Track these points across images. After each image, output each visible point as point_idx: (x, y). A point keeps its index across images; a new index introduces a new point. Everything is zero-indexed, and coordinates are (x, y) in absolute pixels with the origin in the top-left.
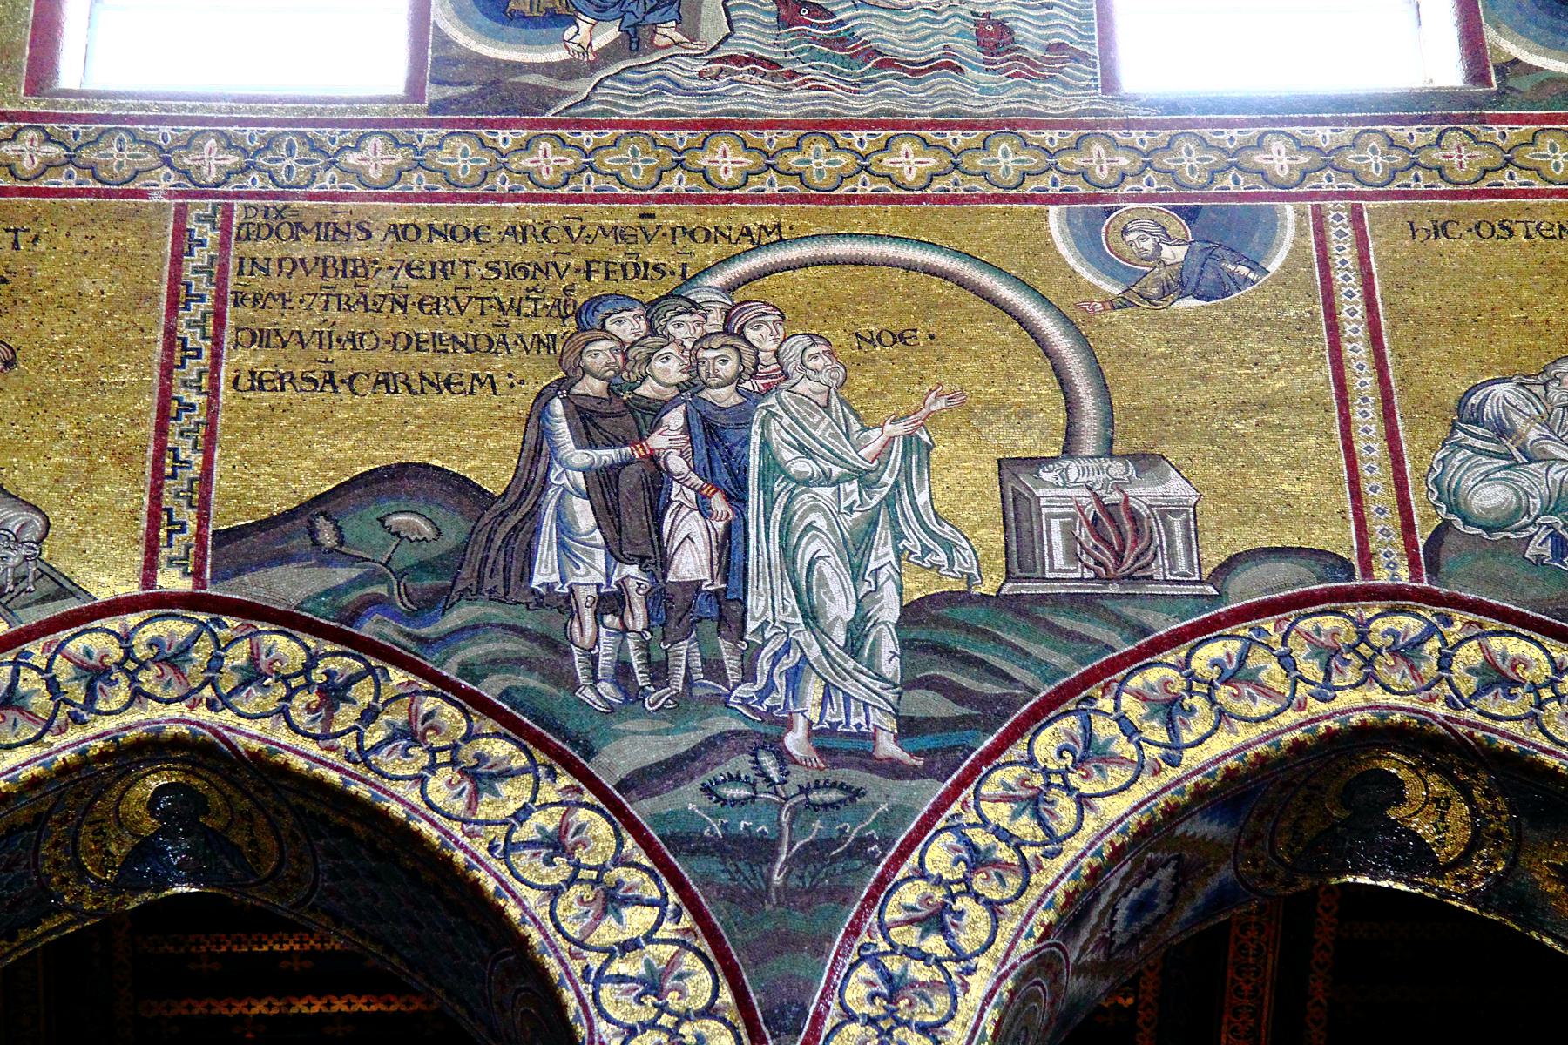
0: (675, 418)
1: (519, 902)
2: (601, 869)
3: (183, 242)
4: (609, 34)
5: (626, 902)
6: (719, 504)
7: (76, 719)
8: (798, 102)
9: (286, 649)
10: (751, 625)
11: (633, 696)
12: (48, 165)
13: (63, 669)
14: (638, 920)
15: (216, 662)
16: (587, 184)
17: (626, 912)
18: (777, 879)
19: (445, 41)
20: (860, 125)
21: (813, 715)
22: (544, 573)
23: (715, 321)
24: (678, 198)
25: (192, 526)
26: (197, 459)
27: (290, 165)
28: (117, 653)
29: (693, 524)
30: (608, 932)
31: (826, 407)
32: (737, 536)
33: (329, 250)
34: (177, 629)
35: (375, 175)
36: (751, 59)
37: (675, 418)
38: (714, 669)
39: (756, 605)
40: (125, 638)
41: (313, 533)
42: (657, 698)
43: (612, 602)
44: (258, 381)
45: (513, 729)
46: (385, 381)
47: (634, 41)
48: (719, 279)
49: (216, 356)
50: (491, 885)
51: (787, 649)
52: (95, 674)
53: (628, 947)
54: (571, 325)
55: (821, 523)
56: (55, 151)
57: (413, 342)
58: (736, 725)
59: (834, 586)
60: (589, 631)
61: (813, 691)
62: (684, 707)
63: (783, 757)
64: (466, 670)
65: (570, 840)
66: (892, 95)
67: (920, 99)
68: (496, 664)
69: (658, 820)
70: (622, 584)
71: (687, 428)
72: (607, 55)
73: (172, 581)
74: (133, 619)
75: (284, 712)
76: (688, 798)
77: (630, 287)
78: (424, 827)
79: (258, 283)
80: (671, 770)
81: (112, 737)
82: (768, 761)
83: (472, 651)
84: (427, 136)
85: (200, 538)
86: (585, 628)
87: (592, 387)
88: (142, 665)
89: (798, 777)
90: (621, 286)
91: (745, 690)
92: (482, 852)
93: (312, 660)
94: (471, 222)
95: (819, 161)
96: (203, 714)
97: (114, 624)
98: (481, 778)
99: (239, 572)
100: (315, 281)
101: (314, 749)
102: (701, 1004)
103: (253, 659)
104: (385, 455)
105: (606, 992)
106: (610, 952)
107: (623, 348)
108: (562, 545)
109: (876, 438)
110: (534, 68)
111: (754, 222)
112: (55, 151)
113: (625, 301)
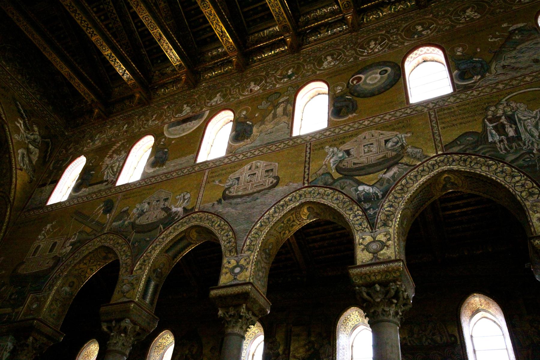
0: (503, 117)
1: (499, 179)
2: (510, 173)
3: (430, 115)
4: (479, 77)
5: (516, 176)
6: (513, 126)
7: (432, 171)
8: (508, 77)
9: (456, 157)
10: (523, 139)
11: (508, 152)
12: (411, 112)
13: (429, 166)
14: (517, 179)
15: (448, 161)
16: (482, 94)
17: (516, 178)
18: (538, 169)
19: (457, 84)
20: (519, 77)
21: (536, 147)
22: (490, 140)
23: (505, 105)
24: (495, 92)
25: (440, 146)
26: (439, 138)
27: (441, 103)
28: (435, 162)
29: (510, 129)
30: (514, 180)
31: (526, 110)
32: (517, 129)
33: (448, 111)
34: (442, 158)
35: (452, 101)
36: (501, 74)
37: (503, 117)
38: (519, 145)
39: (523, 136)
40: (436, 160)
41: (457, 143)
42: (512, 151)
43: (501, 141)
44: (444, 128)
45: (491, 159)
46: (461, 123)
47: (483, 77)
48: (504, 100)
49: (438, 126)
50: (494, 178)
51: (530, 140)
52: (433, 165)
53: (518, 182)
54: (485, 111)
55: (530, 124)
56: (412, 110)
57: (463, 118)
58: (525, 152)
59: (534, 131)
60: (499, 145)
61: (536, 145)
62: (516, 151)
63: (533, 154)
64: (483, 154)
65: (504, 171)
66: (523, 72)
67: (528, 71)
68: (486, 152)
69: (517, 165)
70: (502, 138)
71: (505, 118)
72: (480, 79)
73: (440, 153)
74: (436, 158)
75: (459, 164)
76: (521, 162)
77: (492, 104)
78: (483, 173)
79: (441, 117)
80: (517, 159)
81: (438, 172)
82: (531, 155)
83: (483, 151)
84: (458, 95)
85: (442, 147)
86: (498, 145)
87: (490, 117)
88: (439, 163)
89: (536, 156)
90: (490, 104)
91: (524, 147)
92: (492, 175)
93: (461, 157)
94: (467, 103)
95: (514, 82)
96: (449, 167)
97: (434, 159)
98: (489, 166)
99: (448, 149)
100: (448, 115)
101: (464, 168)
102: (531, 186)
103: (453, 159)
104: (463, 132)
105: (516, 188)
106: (515, 183)
107: (493, 111)
108: (492, 136)
109: (535, 112)
110: (470, 83)
111: (507, 92)
112: (412, 110)
113: (491, 106)
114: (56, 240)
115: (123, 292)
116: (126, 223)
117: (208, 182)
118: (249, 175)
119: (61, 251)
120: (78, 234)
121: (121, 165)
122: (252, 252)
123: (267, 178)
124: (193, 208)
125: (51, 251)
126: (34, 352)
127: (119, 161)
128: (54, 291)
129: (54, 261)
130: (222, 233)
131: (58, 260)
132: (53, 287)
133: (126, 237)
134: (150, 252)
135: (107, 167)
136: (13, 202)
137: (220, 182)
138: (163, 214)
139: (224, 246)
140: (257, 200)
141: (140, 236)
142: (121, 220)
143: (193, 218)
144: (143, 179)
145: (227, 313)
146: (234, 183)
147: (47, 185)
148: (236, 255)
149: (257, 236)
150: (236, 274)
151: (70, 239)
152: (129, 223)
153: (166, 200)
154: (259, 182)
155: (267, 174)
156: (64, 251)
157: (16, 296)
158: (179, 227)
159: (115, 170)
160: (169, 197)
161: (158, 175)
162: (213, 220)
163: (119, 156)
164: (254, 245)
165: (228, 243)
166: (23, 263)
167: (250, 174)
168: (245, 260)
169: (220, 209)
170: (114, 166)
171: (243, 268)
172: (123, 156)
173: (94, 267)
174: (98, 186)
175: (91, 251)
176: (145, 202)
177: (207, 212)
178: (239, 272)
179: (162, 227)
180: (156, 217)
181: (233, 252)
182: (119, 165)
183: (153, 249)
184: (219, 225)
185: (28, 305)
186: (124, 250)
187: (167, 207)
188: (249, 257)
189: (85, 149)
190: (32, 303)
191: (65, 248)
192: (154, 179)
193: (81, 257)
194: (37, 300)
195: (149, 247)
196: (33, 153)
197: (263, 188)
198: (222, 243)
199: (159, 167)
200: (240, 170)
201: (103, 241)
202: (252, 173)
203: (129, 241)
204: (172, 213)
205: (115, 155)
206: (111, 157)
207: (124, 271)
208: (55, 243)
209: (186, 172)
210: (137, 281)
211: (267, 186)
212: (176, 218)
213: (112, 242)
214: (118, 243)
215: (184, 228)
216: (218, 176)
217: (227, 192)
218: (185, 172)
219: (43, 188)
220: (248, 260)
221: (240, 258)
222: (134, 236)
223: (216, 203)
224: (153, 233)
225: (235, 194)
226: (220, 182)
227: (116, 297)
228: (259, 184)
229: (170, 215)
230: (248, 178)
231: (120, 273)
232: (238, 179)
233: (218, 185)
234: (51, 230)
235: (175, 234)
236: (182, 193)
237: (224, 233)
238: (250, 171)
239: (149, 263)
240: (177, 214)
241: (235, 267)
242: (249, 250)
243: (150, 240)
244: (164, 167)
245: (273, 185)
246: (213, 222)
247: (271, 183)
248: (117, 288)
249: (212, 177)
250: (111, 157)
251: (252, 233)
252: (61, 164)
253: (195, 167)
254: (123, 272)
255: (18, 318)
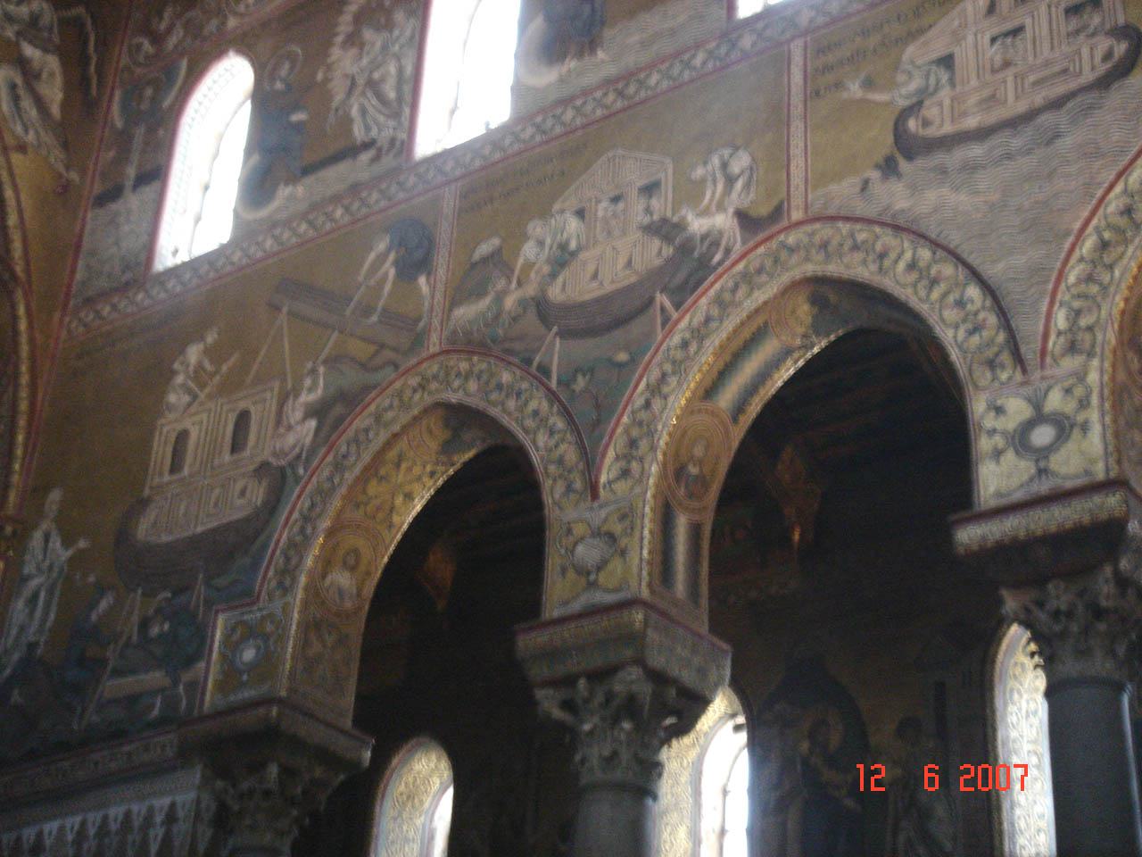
114: (242, 405)
115: (582, 571)
116: (509, 302)
117: (813, 94)
118: (993, 40)
119: (278, 446)
120: (322, 369)
121: (409, 70)
122: (1091, 355)
123: (1082, 37)
124: (777, 213)
125: (237, 446)
126: (295, 813)
127: (398, 58)
128: (300, 594)
129: (264, 483)
130: (935, 295)
131: (278, 479)
132: (294, 580)
133: (528, 362)
134: (647, 405)
135: (353, 84)
136: (29, 281)
137: (869, 84)
138: (654, 253)
139: (960, 347)
140: (1059, 143)
141: (585, 349)
142: (480, 293)
143: (792, 250)
144: (522, 118)
145: (1040, 604)
146: (932, 81)
147: (127, 191)
148: (1019, 376)
149: (1094, 289)
150: (1044, 453)
151: (296, 392)
152: (523, 303)
153: (650, 189)
154: (1047, 64)
155: (1074, 23)
156: (291, 439)
157: (166, 626)
158: (740, 294)
159: (392, 95)
160: (662, 176)
161: (586, 92)
162: (879, 247)
163: (385, 34)
164: (1090, 329)
165: (971, 333)
166: (144, 503)
167: (996, 31)
168: (1068, 391)
169: (896, 196)
170: (383, 80)
171: (1064, 427)
172: (408, 33)
173: (416, 487)
174: (342, 167)
175: (396, 428)
176: (562, 211)
177: (847, 219)
178: (1052, 445)
179: (668, 304)
180: (629, 263)
181: (1003, 367)
182: (400, 71)
183: (656, 390)
184: (912, 266)
185: (223, 655)
186: (536, 413)
187: (664, 221)
188: (1081, 377)
189: (232, 22)
190: (232, 646)
191: (290, 428)
192: (569, 114)
193: (366, 457)
194: (252, 632)
195: (636, 387)
196: (44, 75)
197: (1073, 85)
198: (947, 336)
199: (580, 55)
200: (952, 20)
201: (434, 386)
202: (1008, 26)
203: (544, 370)
204: (690, 239)
205: (368, 34)
206: (353, 40)
207: (560, 488)
208: (243, 419)
209: (704, 63)
210: (627, 522)
211: (1088, 76)
212: (717, 258)
213: (473, 386)
214: (499, 387)
215: (761, 296)
216: (851, 59)
217: (912, 124)
218: (698, 61)
219: (113, 207)
220: (1079, 391)
221: (1044, 385)
222: (556, 352)
223: (875, 175)
224: (636, 329)
225: (948, 128)
226: (869, 84)
227: (559, 593)
228: (1047, 72)
229: (685, 249)
230: (994, 53)
231: (548, 500)
232: (947, 62)
233: (863, 102)
234: (208, 366)
235: (729, 325)
236: (710, 152)
237: (945, 295)
238: (994, 19)
239: (653, 448)
240: (715, 244)
241: (1029, 426)
242: (1072, 348)
243: (633, 361)
244: (601, 54)
245: (1115, 67)
246: (882, 256)
247: (1108, 55)
248: (553, 560)
249: (827, 68)
250: (353, 40)
251: (1072, 279)
252: (155, 100)
253: (740, 36)
254: (557, 496)
255: (202, 701)
